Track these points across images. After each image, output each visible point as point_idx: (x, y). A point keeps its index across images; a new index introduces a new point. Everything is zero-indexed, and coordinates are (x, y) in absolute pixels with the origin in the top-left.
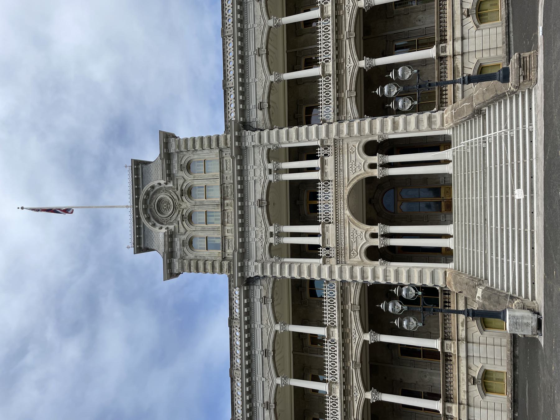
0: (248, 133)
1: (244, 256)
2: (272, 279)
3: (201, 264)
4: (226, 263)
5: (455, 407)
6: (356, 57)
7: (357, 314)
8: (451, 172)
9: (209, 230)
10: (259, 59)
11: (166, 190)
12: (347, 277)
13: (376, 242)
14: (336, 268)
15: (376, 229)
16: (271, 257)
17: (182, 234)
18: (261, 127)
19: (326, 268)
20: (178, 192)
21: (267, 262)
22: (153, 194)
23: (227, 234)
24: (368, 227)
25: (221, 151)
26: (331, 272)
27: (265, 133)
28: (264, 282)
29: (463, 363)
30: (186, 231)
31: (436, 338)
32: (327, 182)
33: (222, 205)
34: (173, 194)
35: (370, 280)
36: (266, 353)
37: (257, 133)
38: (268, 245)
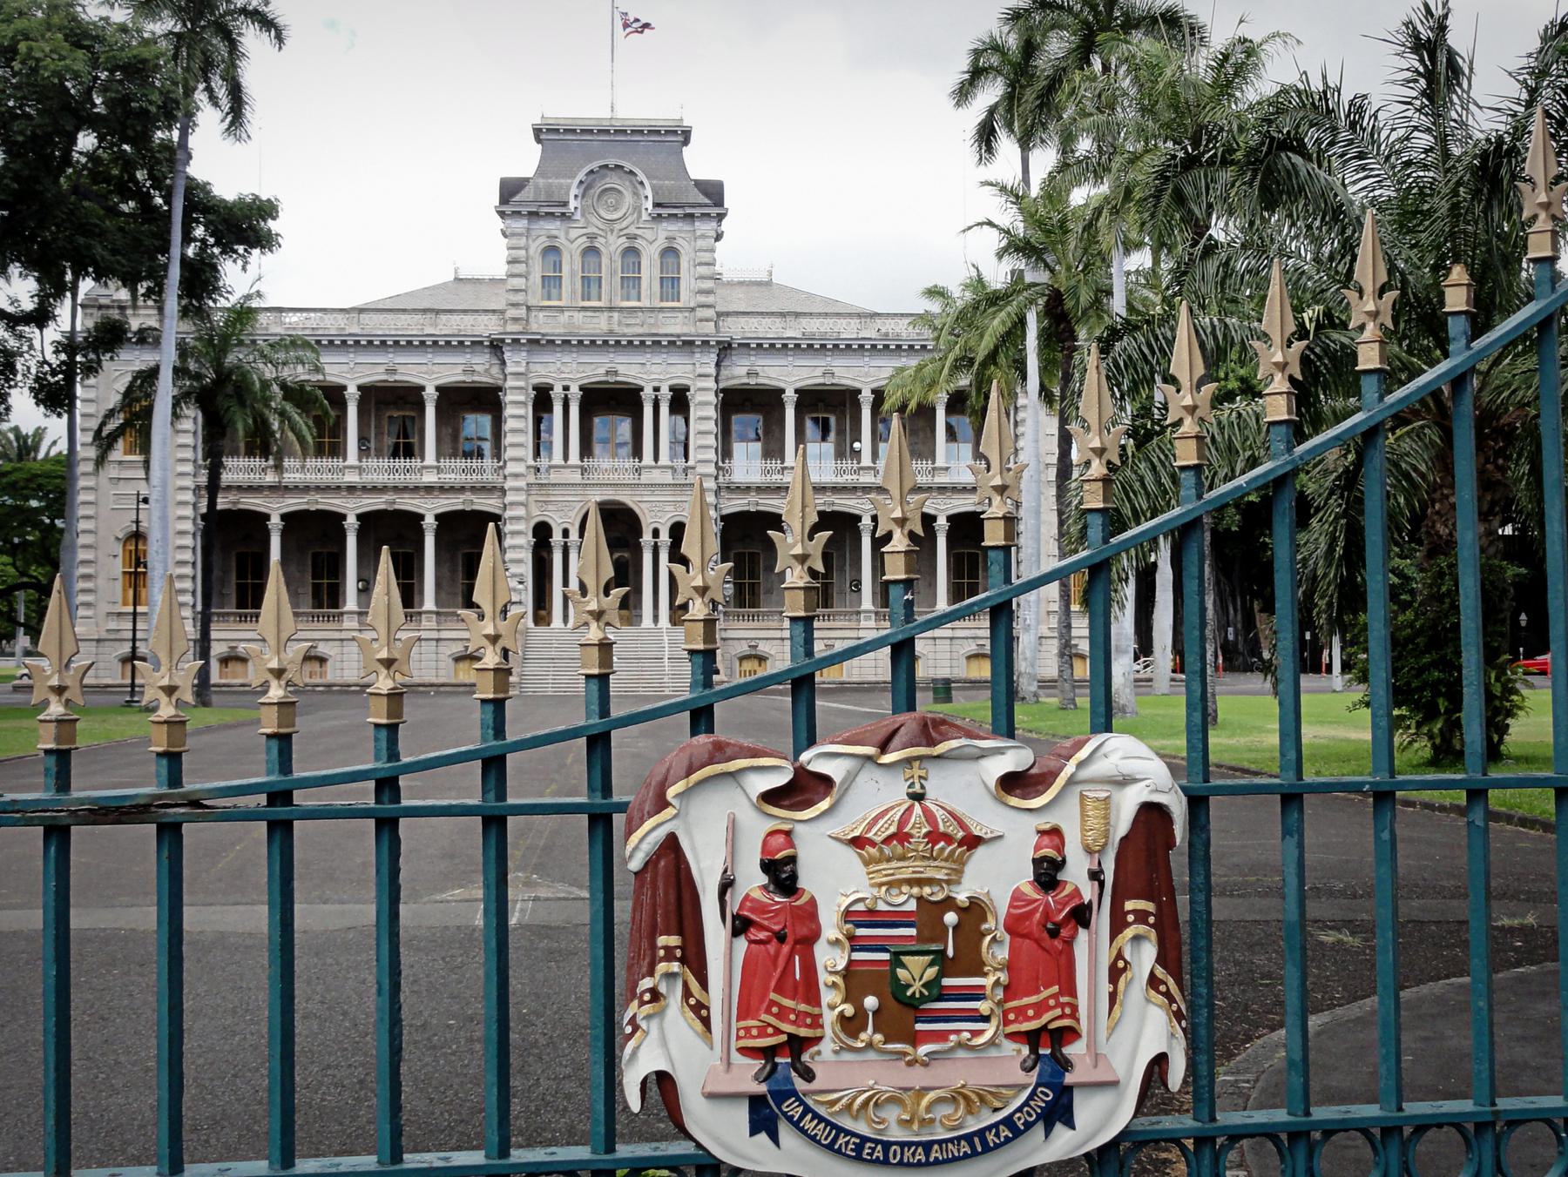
0: (714, 357)
1: (536, 344)
2: (500, 383)
3: (521, 268)
4: (522, 312)
7: (460, 507)
8: (643, 625)
9: (573, 283)
10: (819, 372)
11: (637, 209)
12: (510, 498)
13: (557, 537)
14: (521, 483)
17: (567, 233)
18: (724, 373)
19: (519, 468)
20: (632, 230)
21: (527, 380)
23: (567, 314)
25: (693, 309)
26: (516, 476)
27: (711, 384)
28: (495, 370)
31: (437, 603)
32: (638, 471)
33: (611, 309)
34: (629, 220)
36: (393, 371)
37: (712, 370)
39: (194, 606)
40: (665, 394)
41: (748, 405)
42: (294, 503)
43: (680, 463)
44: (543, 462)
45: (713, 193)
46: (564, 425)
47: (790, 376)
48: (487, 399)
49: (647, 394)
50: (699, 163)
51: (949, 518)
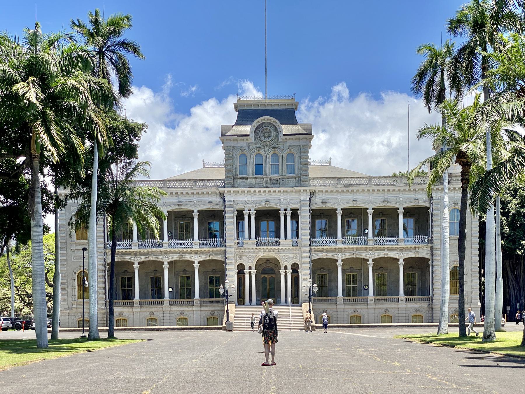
6: (343, 258)
18: (312, 202)
22: (274, 125)
23: (249, 180)
29: (191, 309)
30: (251, 150)
33: (267, 178)
35: (228, 267)
39: (106, 299)
40: (289, 212)
41: (323, 216)
42: (143, 258)
43: (295, 239)
44: (240, 240)
46: (249, 225)
48: (218, 216)
49: (282, 212)
51: (404, 260)
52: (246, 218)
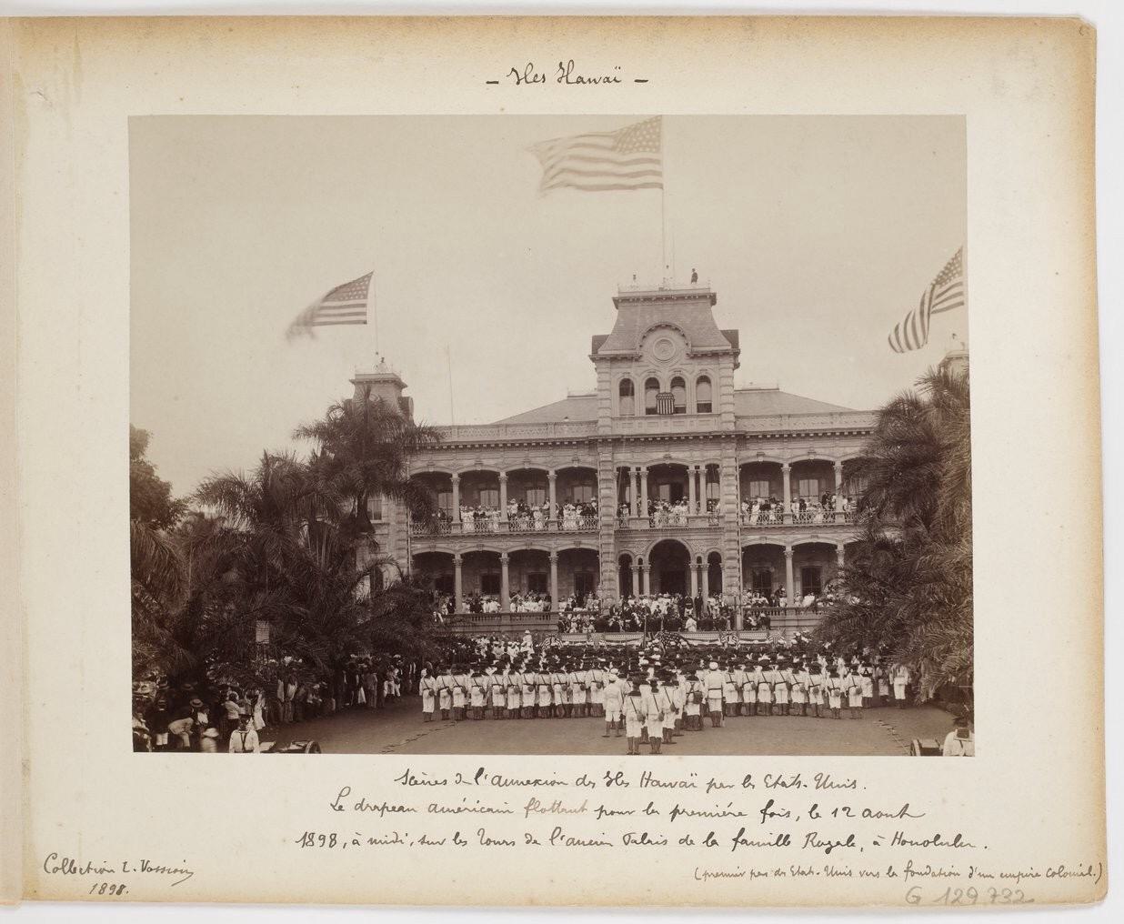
4: (608, 421)
5: (508, 622)
10: (804, 452)
13: (635, 564)
15: (646, 565)
16: (618, 469)
24: (647, 557)
38: (628, 465)
40: (703, 468)
45: (732, 337)
46: (638, 495)
47: (785, 455)
48: (586, 477)
49: (692, 468)
50: (722, 318)
52: (633, 482)
